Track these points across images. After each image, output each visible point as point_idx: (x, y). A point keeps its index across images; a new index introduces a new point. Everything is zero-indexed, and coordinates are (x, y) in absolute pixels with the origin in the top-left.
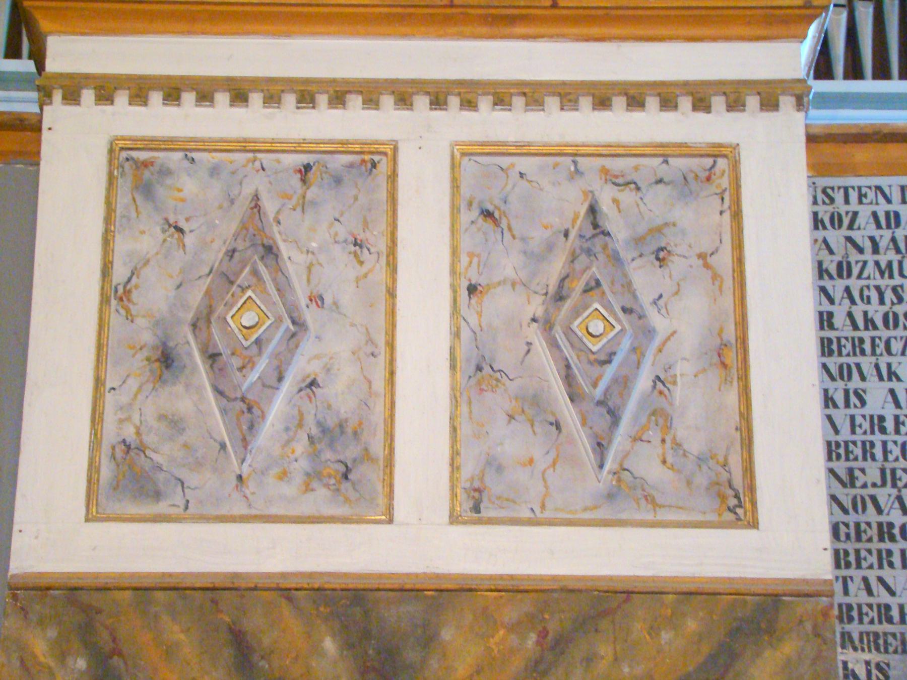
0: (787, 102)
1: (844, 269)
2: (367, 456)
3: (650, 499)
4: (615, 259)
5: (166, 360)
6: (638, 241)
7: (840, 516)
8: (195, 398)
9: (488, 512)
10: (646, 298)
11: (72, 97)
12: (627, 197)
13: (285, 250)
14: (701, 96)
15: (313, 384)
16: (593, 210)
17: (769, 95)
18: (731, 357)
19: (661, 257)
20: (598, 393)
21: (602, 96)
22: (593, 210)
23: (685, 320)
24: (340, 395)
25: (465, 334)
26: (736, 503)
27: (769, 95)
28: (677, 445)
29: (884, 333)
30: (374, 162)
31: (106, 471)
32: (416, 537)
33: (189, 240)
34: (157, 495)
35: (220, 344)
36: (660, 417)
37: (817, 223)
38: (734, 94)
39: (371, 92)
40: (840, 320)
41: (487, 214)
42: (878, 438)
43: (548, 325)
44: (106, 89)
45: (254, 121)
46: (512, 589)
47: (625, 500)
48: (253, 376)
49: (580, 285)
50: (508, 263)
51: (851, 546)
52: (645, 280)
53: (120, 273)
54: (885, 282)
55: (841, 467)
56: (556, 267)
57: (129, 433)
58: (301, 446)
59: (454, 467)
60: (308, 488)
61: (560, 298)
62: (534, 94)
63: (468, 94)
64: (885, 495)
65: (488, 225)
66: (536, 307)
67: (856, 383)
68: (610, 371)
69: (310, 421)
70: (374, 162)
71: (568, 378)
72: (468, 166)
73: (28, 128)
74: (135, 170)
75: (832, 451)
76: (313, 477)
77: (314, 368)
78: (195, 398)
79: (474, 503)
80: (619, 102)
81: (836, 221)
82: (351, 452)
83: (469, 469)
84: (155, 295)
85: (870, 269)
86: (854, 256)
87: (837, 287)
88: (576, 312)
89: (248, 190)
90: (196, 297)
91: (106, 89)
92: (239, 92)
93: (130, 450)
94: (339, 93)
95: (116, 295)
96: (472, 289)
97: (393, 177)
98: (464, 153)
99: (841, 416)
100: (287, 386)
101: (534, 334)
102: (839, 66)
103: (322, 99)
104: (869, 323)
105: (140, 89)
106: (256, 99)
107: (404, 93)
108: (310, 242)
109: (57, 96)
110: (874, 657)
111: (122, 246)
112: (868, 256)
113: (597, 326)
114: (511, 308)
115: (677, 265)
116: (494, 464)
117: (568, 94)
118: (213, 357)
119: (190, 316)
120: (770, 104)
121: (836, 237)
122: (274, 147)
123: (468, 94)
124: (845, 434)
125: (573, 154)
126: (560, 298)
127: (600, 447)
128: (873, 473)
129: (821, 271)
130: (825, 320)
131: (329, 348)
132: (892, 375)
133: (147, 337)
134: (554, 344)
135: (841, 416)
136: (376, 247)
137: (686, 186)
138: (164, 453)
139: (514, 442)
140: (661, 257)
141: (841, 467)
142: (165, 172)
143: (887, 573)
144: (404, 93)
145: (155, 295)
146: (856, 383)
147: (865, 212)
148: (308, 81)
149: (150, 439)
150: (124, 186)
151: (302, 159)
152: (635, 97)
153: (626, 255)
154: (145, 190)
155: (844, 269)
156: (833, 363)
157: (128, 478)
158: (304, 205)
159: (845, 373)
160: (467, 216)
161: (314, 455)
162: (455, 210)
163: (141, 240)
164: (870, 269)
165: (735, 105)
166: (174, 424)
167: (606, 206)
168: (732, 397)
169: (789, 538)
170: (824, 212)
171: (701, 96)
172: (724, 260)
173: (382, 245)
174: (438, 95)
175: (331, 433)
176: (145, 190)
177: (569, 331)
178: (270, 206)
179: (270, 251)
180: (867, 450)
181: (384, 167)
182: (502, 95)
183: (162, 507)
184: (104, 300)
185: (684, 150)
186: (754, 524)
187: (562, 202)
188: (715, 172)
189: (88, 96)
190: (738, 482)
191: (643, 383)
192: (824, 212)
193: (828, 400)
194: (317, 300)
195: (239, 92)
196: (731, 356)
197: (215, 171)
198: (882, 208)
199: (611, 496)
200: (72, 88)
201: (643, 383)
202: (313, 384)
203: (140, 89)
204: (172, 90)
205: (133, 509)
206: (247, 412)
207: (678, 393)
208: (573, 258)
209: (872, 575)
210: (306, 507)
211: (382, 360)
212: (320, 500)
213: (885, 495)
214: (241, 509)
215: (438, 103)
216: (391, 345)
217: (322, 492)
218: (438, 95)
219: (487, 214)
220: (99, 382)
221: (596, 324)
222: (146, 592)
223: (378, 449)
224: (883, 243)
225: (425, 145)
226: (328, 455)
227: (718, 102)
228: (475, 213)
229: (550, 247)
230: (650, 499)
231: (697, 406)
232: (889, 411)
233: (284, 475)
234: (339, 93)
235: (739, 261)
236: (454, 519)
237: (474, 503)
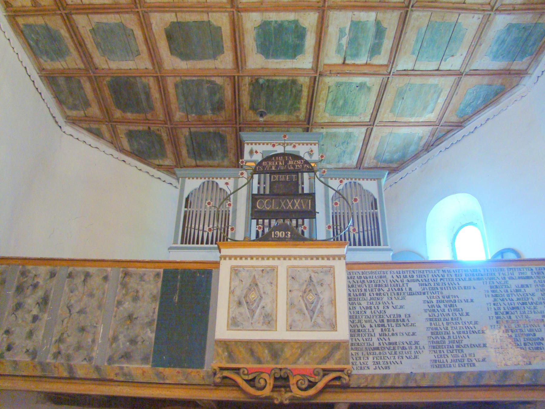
0: (342, 258)
1: (352, 286)
2: (273, 319)
3: (319, 326)
4: (314, 285)
5: (240, 303)
6: (318, 282)
7: (351, 328)
8: (244, 310)
9: (292, 329)
10: (319, 292)
11: (225, 259)
12: (316, 274)
13: (259, 284)
14: (328, 257)
15: (264, 307)
16: (310, 277)
17: (340, 257)
18: (333, 302)
19: (322, 285)
20: (311, 309)
21: (312, 257)
22: (310, 277)
23: (325, 296)
24: (268, 309)
25: (289, 299)
26: (333, 327)
27: (340, 257)
28: (324, 317)
29: (359, 297)
30: (274, 269)
31: (230, 322)
32: (280, 334)
33: (244, 283)
34: (238, 326)
35: (248, 300)
36: (321, 312)
37: (348, 278)
38: (334, 257)
39: (273, 257)
40: (352, 295)
41: (293, 278)
42: (358, 315)
43: (303, 297)
44: (230, 257)
45: (254, 262)
46: (296, 342)
47: (316, 327)
48: (254, 306)
49: (308, 290)
50: (296, 286)
51: (353, 333)
52: (319, 289)
53: (232, 288)
54: (359, 288)
55: (352, 320)
56: (304, 287)
57: (234, 316)
58: (262, 318)
59: (287, 321)
60: (263, 325)
61: (305, 292)
62: (300, 257)
63: (290, 257)
64: (359, 324)
65: (292, 280)
66: (301, 294)
67: (354, 305)
68: (313, 305)
69: (263, 313)
70: (274, 269)
71: (306, 306)
72: (290, 270)
73: (217, 263)
74: (235, 271)
75: (350, 317)
76: (264, 323)
77: (264, 305)
78: (244, 310)
79: (290, 328)
80: (315, 259)
81: (351, 278)
82: (270, 319)
83: (289, 322)
84: (238, 292)
85: (357, 286)
86: (354, 284)
87: (351, 289)
88: (307, 295)
89: (253, 274)
90: (245, 292)
91: (230, 257)
92: (252, 258)
93: (234, 318)
94: (268, 257)
95: (232, 292)
96: (290, 291)
97: (277, 272)
98: (289, 267)
99: (352, 311)
100: (259, 308)
101: (301, 299)
102: (357, 243)
103: (266, 259)
104: (357, 295)
105: (236, 257)
106: (255, 259)
108: (263, 283)
109: (223, 259)
110: (356, 352)
111: (233, 283)
112: (356, 284)
113: (311, 297)
114: (297, 294)
115: (324, 286)
116: (294, 321)
117: (306, 257)
118: (247, 303)
119: (243, 296)
120: (340, 259)
121: (351, 280)
122: (258, 267)
123: (290, 257)
124: (352, 314)
125: (307, 267)
126: (305, 292)
127: (311, 318)
128: (357, 321)
129: (349, 286)
130: (349, 295)
131: (266, 301)
132: (360, 304)
133: (236, 299)
134: (304, 300)
135: (352, 311)
136: (274, 283)
137: (326, 273)
138: (239, 319)
139: (297, 317)
140: (322, 285)
141: (352, 320)
142: (240, 271)
143: (359, 338)
145: (238, 292)
146: (354, 305)
147: (356, 276)
148: (263, 256)
149: (237, 317)
150: (233, 273)
151: (262, 269)
152: (317, 257)
153: (316, 285)
154: (236, 274)
155: (352, 286)
156: (351, 302)
157: (234, 323)
158: (262, 277)
159: (352, 304)
160: (289, 278)
161: (264, 319)
162: (287, 277)
163: (236, 283)
164: (357, 286)
165: (334, 259)
166: (241, 314)
167: (313, 276)
168: (333, 309)
169: (342, 333)
170: (349, 276)
171: (328, 257)
172: (332, 285)
173: (275, 283)
174: (285, 257)
175: (267, 316)
176: (236, 274)
177: (306, 299)
178: (257, 277)
179: (257, 285)
180: (356, 318)
181: (276, 270)
182: (295, 257)
183: (239, 328)
184: (230, 293)
185: (325, 267)
186: (336, 331)
187: (305, 276)
188: (330, 270)
189: (227, 258)
190: (334, 324)
191: (319, 307)
192: (349, 276)
193: (350, 309)
194: (264, 293)
195: (252, 258)
196: (333, 302)
197: (248, 271)
198: (359, 275)
199: (313, 326)
200: (225, 257)
201: (319, 307)
202: (264, 307)
203: (236, 257)
204: (241, 257)
205: (235, 328)
206: (253, 312)
207: (324, 308)
208: (307, 286)
209: (356, 338)
210: (263, 328)
211: (275, 303)
212: (265, 327)
213: (359, 324)
214: (252, 328)
215: (285, 259)
216: (277, 300)
217: (265, 326)
218: (285, 257)
219: (293, 278)
220: (229, 307)
221: (311, 297)
222: (236, 342)
223: (275, 319)
224: (359, 281)
225: (282, 266)
226: (266, 319)
227: (331, 258)
228: (291, 278)
229: (303, 284)
230: (319, 326)
231: (327, 310)
232: (360, 310)
233: (259, 323)
234: (268, 257)
235: (335, 286)
236: (287, 330)
237: (290, 328)
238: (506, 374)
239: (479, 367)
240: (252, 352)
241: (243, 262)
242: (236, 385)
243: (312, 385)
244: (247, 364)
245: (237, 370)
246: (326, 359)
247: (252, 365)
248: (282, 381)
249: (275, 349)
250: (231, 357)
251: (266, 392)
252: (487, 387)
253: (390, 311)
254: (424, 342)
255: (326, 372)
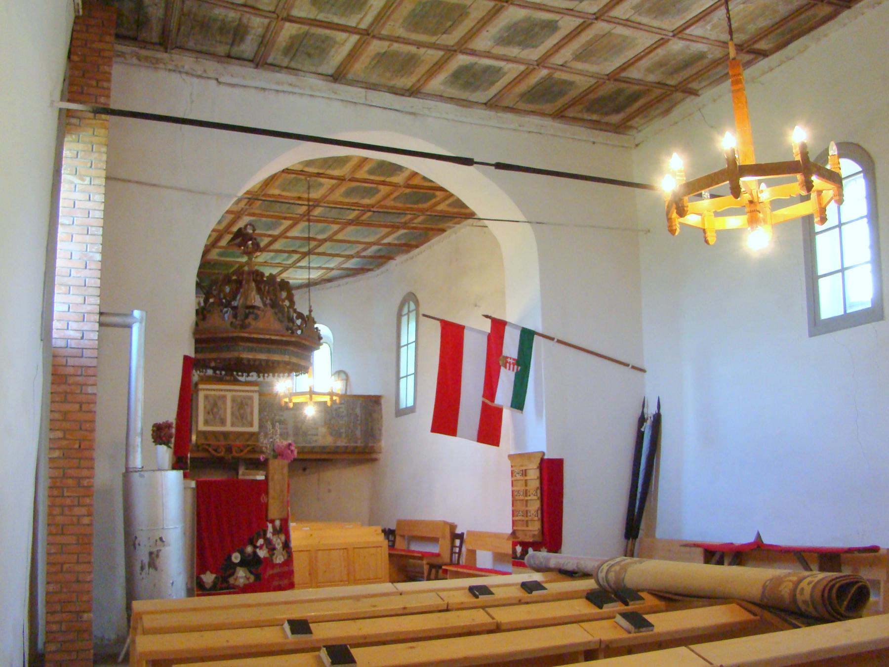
23: (248, 410)
26: (252, 426)
30: (224, 397)
32: (228, 428)
44: (204, 390)
47: (243, 425)
74: (206, 397)
78: (211, 416)
79: (232, 425)
91: (204, 390)
94: (222, 390)
95: (205, 407)
107: (227, 390)
108: (220, 403)
136: (225, 403)
144: (227, 390)
157: (206, 423)
169: (255, 428)
175: (221, 419)
187: (239, 400)
188: (251, 398)
196: (252, 413)
221: (242, 411)
222: (209, 432)
225: (229, 395)
231: (249, 418)
234: (222, 390)
237: (232, 425)
238: (324, 448)
239: (313, 444)
240: (216, 437)
241: (213, 393)
242: (209, 452)
243: (242, 451)
244: (213, 442)
245: (209, 445)
246: (248, 440)
247: (217, 443)
248: (229, 449)
249: (225, 435)
250: (206, 439)
251: (222, 454)
252: (316, 453)
253: (277, 418)
254: (291, 432)
255: (248, 446)
